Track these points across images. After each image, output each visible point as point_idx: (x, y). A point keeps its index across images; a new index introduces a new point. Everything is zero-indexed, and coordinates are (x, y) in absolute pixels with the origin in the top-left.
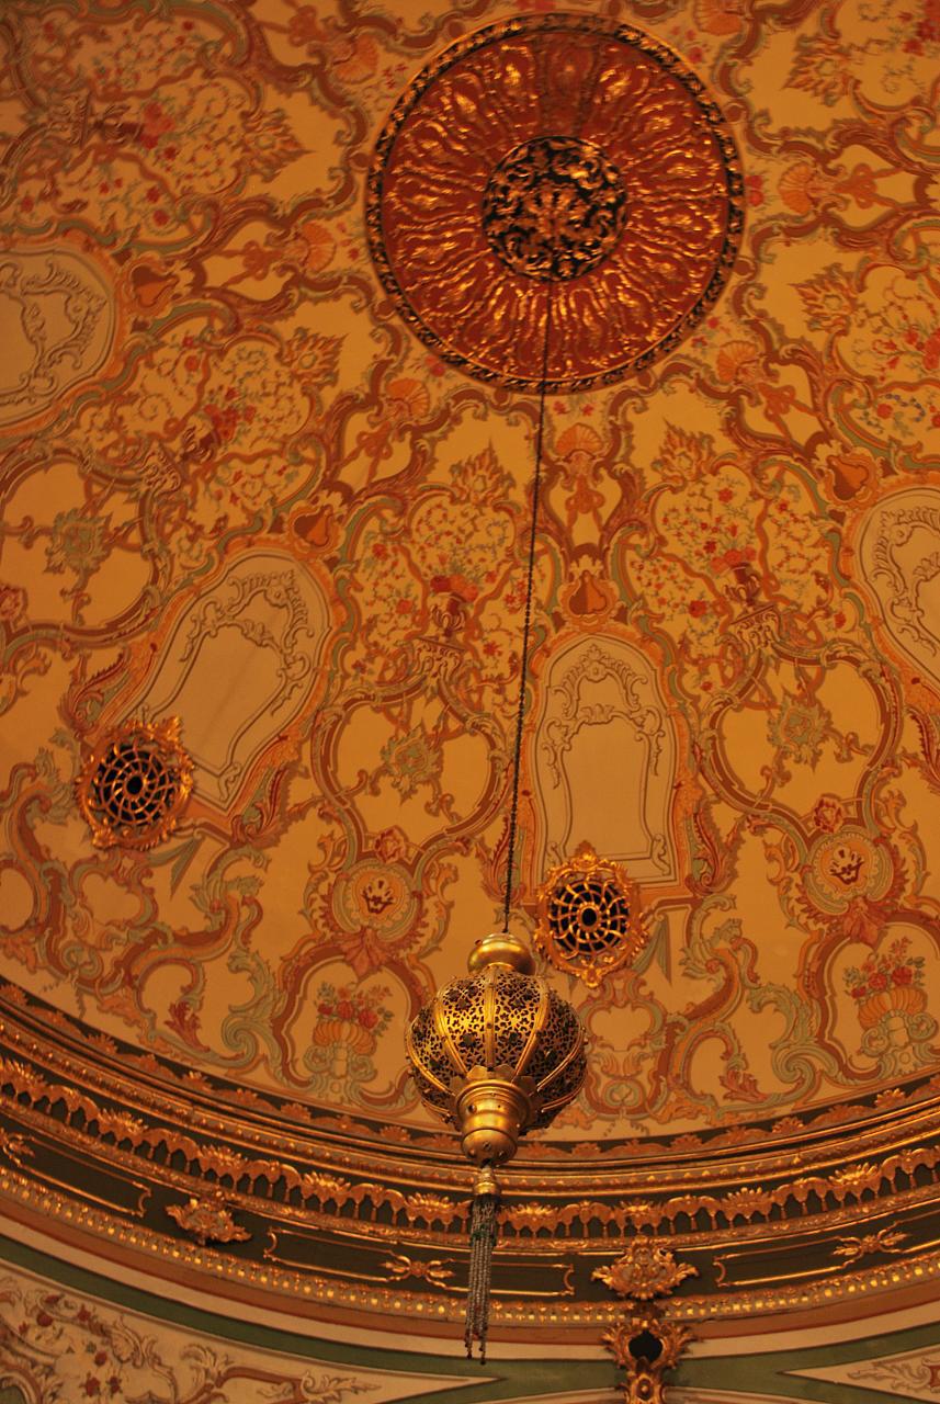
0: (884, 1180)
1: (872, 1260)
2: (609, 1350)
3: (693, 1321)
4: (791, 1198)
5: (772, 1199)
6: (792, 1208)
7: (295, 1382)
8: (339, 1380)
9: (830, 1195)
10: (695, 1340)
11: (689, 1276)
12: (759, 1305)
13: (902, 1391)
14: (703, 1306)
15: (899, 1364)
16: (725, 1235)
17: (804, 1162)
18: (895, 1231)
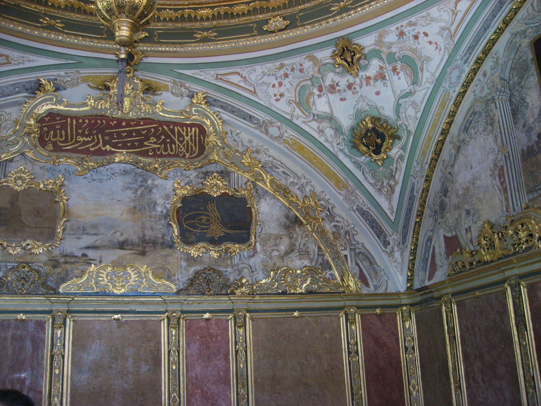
0: (214, 15)
1: (205, 40)
2: (117, 57)
3: (146, 51)
4: (183, 15)
5: (176, 15)
6: (182, 19)
7: (7, 57)
8: (23, 57)
9: (196, 16)
10: (145, 57)
11: (146, 36)
12: (167, 49)
13: (207, 80)
14: (149, 47)
15: (207, 72)
16: (159, 24)
17: (189, 4)
18: (214, 32)
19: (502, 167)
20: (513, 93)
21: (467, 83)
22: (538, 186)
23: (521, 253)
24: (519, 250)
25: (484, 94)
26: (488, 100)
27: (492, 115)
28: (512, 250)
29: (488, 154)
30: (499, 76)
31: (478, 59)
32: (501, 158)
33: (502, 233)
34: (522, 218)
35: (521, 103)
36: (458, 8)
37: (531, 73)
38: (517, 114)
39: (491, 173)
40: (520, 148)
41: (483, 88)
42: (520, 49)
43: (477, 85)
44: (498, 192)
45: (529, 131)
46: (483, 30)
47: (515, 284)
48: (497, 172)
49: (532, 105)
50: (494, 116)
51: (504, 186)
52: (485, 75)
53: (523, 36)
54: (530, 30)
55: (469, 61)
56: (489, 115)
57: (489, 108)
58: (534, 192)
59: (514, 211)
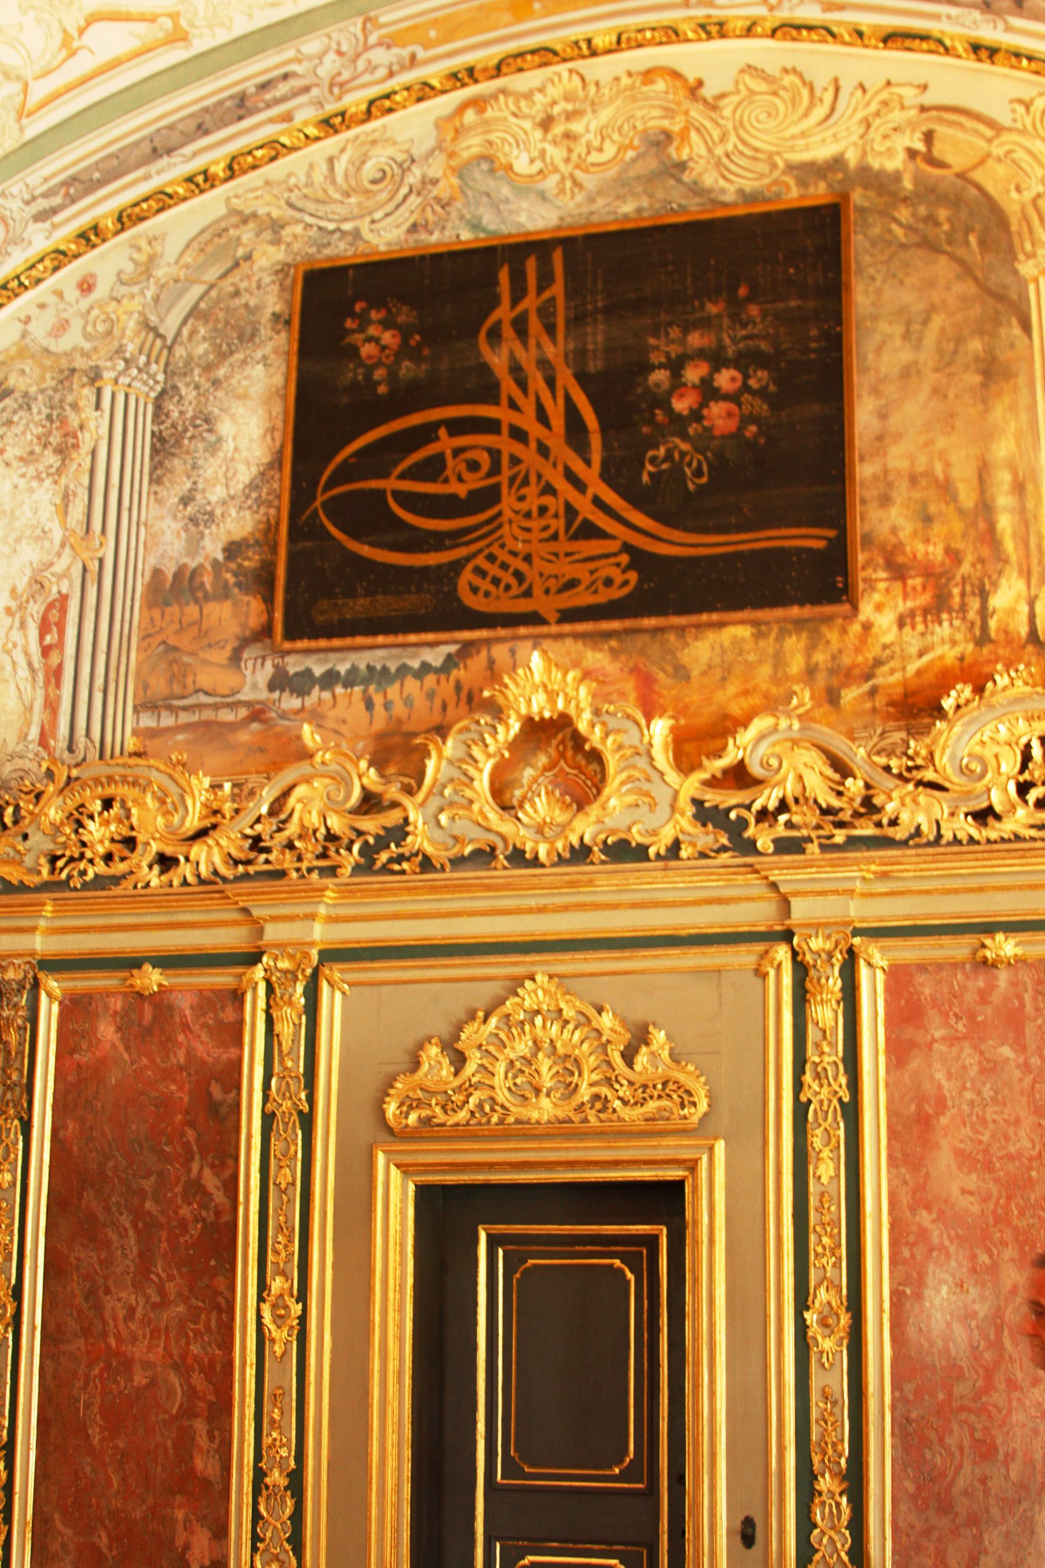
19: (64, 599)
20: (175, 388)
21: (21, 284)
22: (183, 697)
23: (76, 889)
24: (70, 877)
25: (63, 344)
26: (73, 371)
27: (76, 424)
28: (45, 871)
29: (18, 540)
30: (142, 314)
31: (95, 229)
32: (68, 569)
33: (17, 808)
34: (110, 779)
35: (196, 427)
36: (88, 38)
37: (259, 354)
38: (173, 455)
39: (13, 605)
40: (152, 561)
41: (62, 327)
42: (245, 267)
43: (42, 306)
44: (23, 672)
45: (200, 520)
46: (146, 148)
47: (19, 983)
48: (36, 609)
49: (236, 449)
50: (81, 427)
51: (54, 659)
52: (86, 286)
53: (268, 235)
54: (299, 229)
55: (58, 219)
56: (63, 421)
57: (70, 399)
58: (164, 714)
59: (71, 749)
